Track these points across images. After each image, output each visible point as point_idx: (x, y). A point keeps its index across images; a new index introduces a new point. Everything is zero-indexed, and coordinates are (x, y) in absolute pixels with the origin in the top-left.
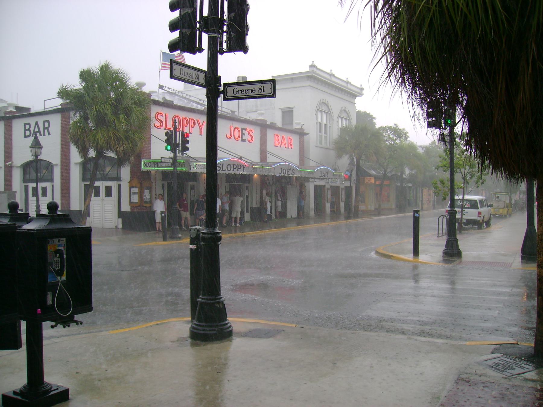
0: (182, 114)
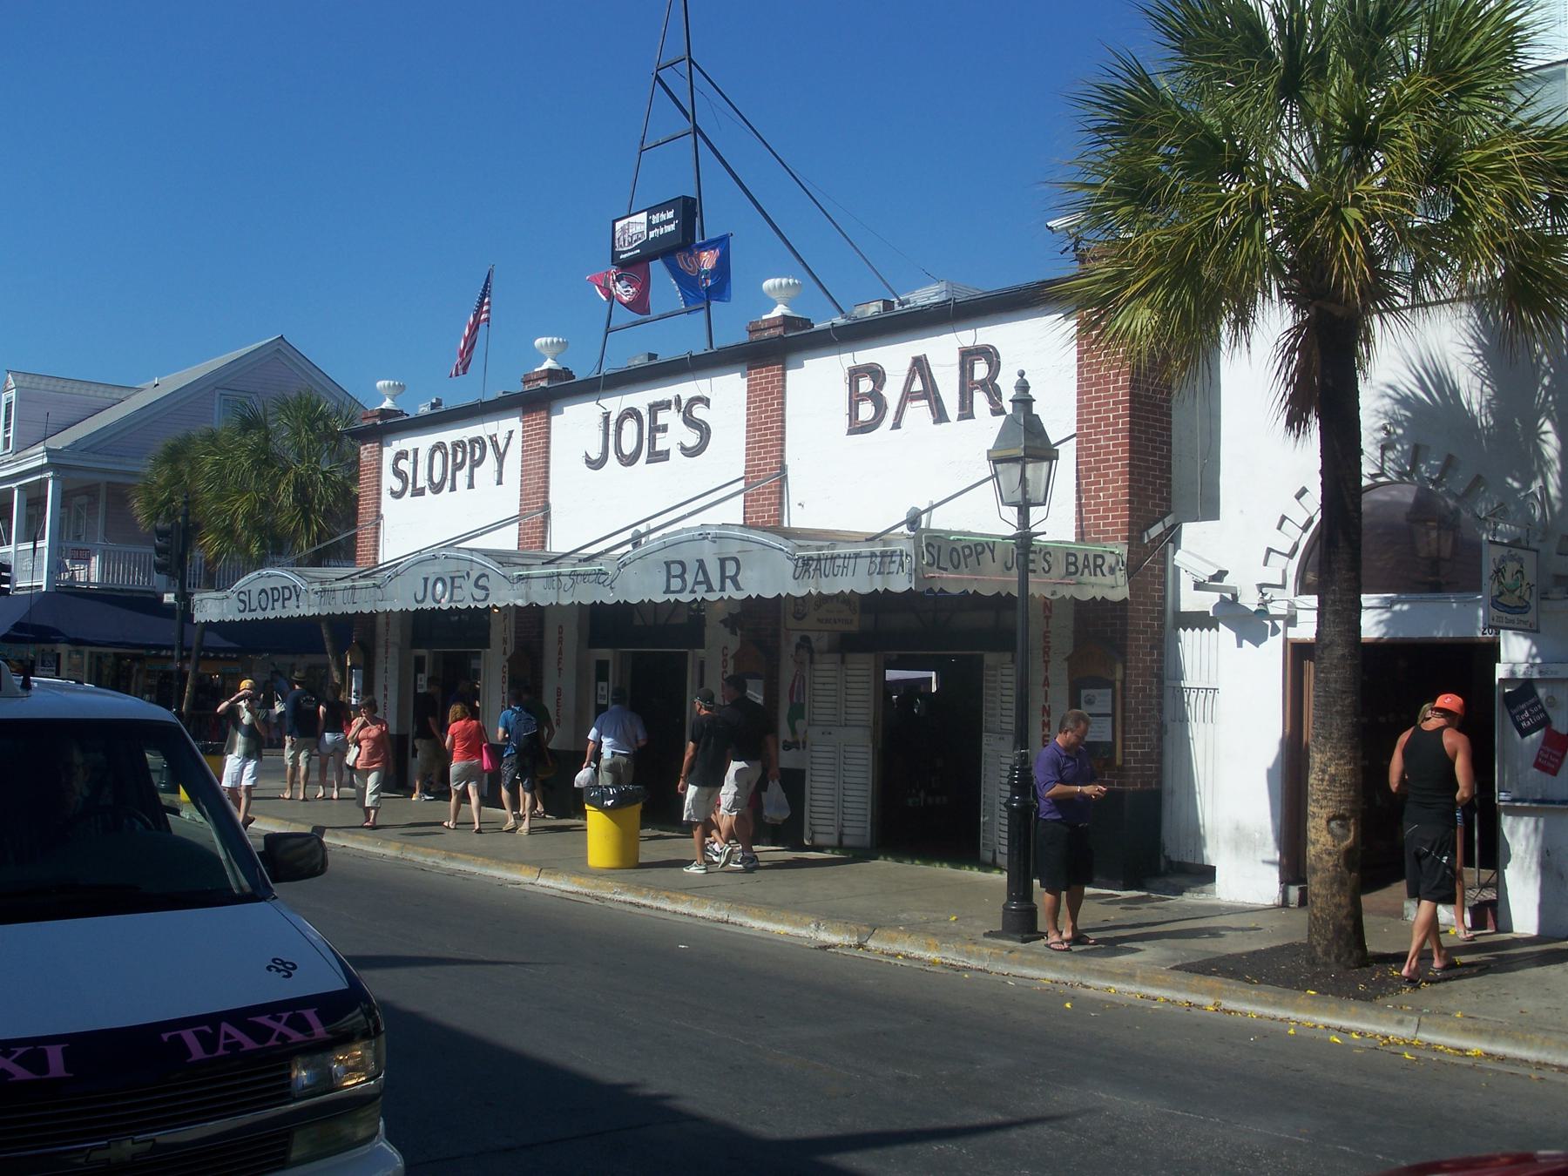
0: (449, 436)
